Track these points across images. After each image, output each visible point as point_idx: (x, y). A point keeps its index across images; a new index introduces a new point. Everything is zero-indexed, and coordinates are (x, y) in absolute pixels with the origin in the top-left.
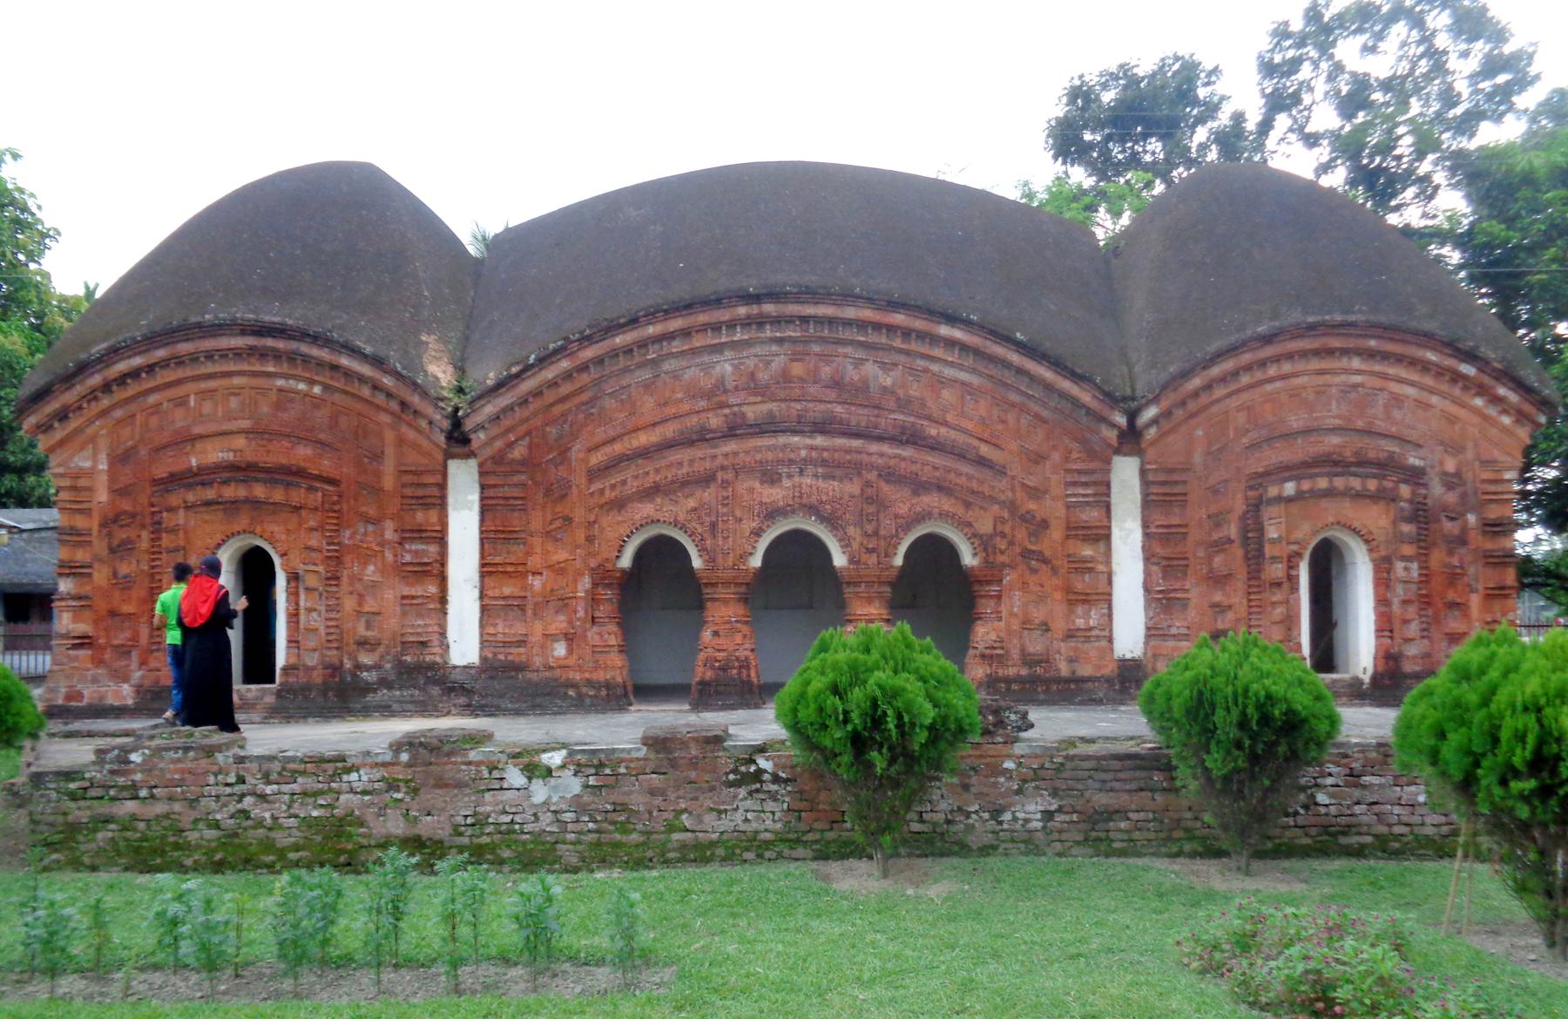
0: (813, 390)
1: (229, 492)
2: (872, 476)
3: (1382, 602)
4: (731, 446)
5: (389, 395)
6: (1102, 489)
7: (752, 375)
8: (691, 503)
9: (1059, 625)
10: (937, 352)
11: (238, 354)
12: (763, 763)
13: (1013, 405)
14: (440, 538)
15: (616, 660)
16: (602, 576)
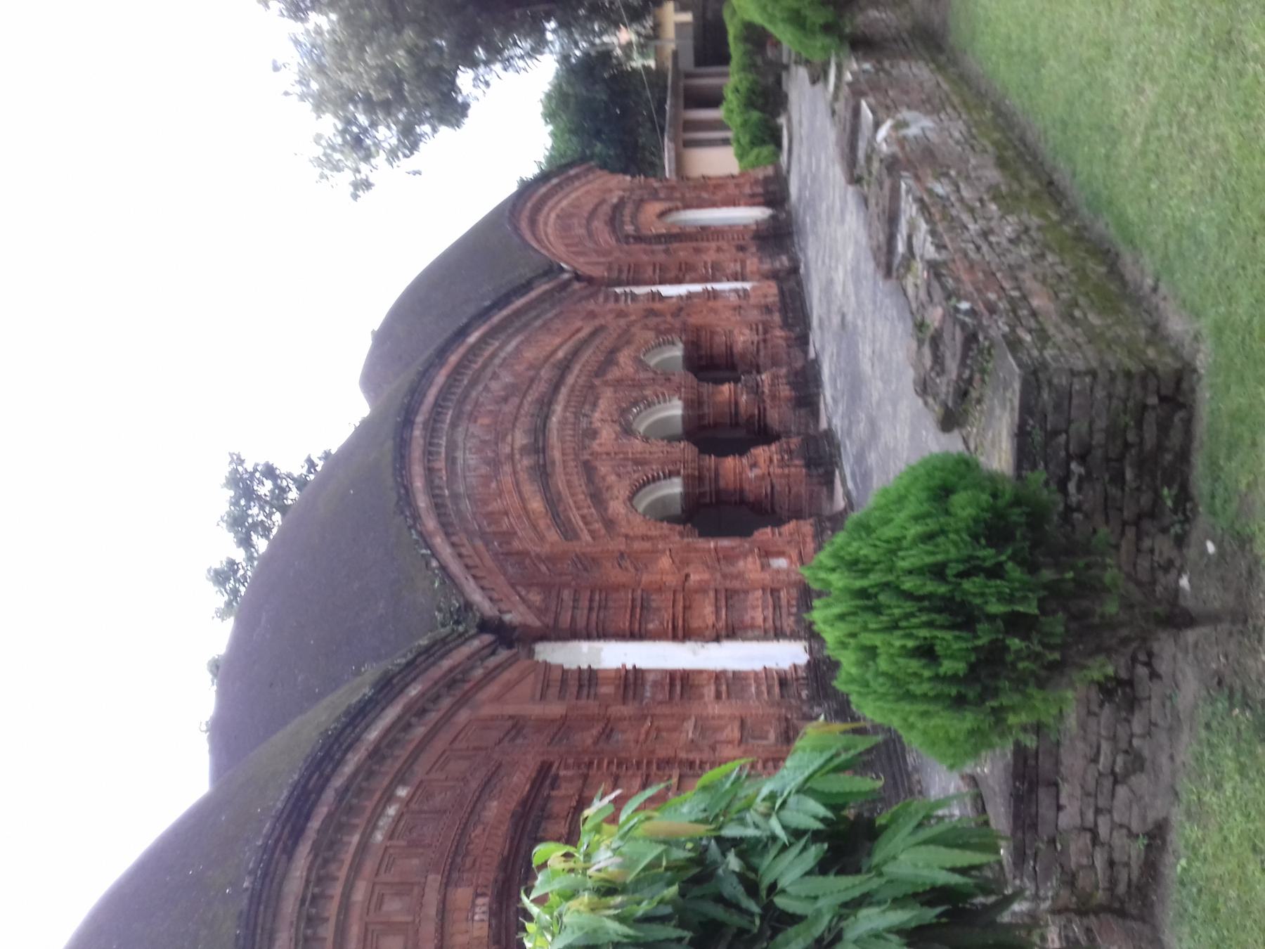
2: (597, 382)
3: (714, 204)
8: (612, 478)
10: (490, 349)
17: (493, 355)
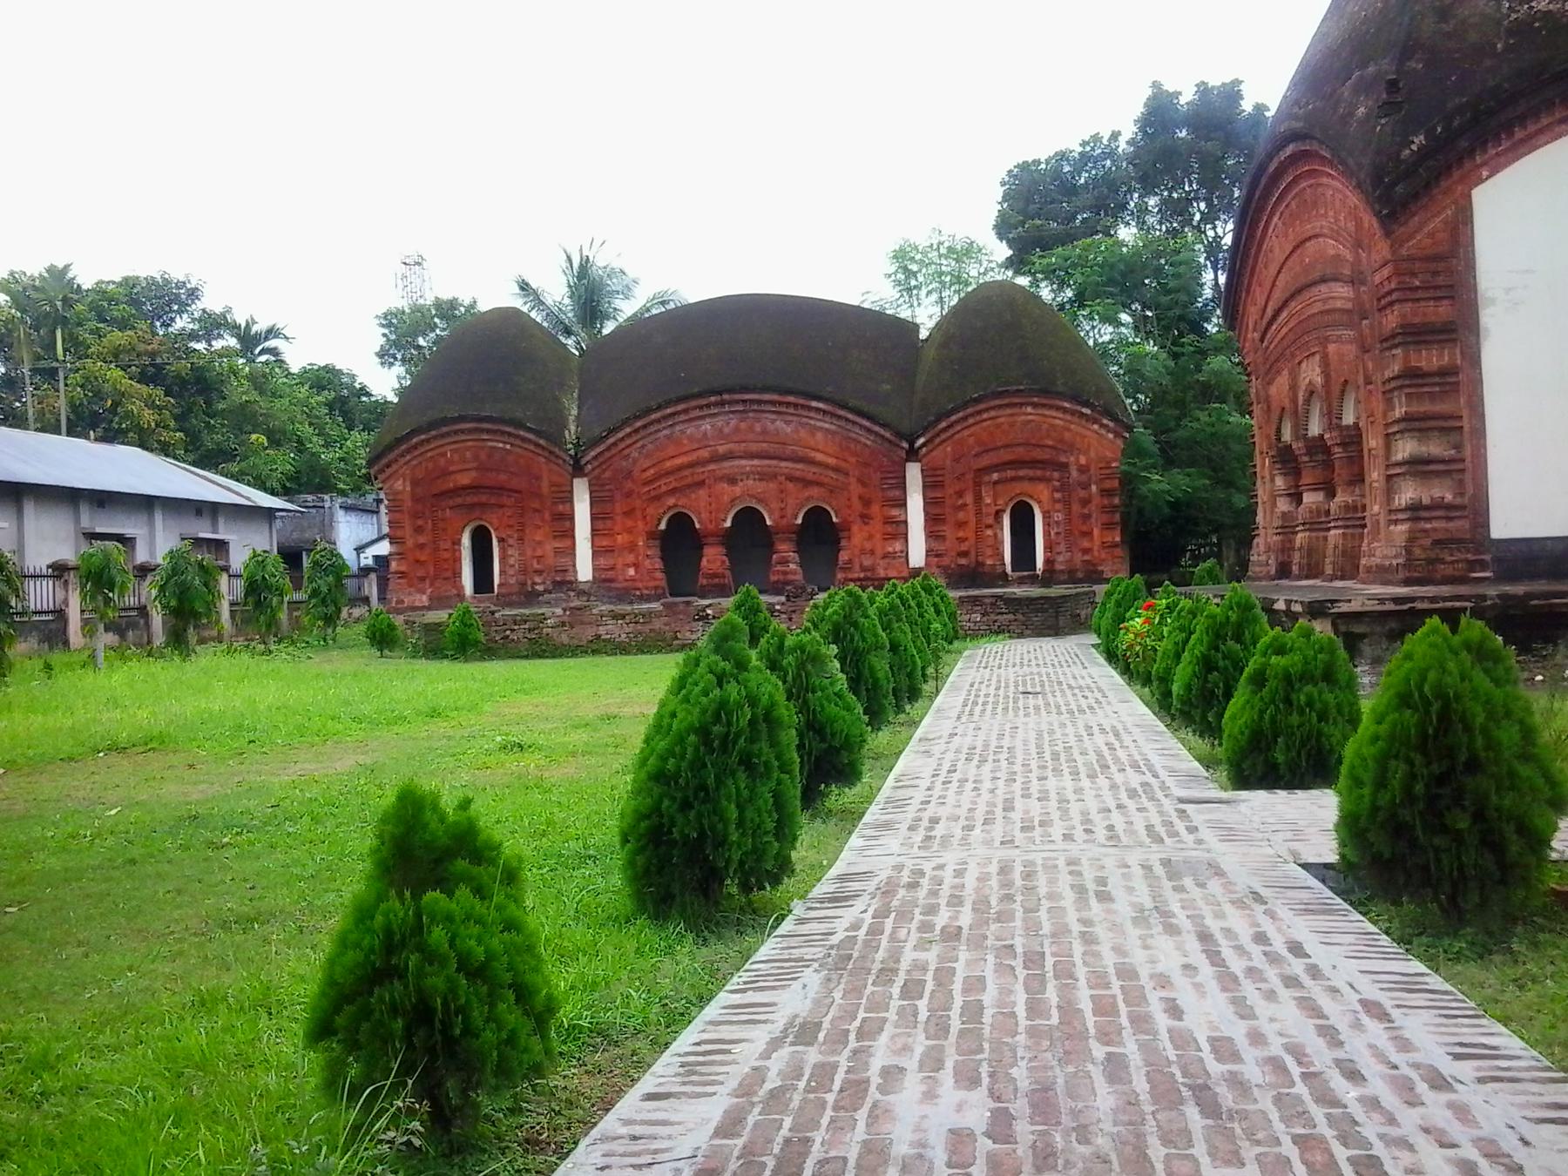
0: (751, 436)
1: (469, 500)
3: (1047, 534)
4: (712, 467)
5: (543, 448)
6: (900, 480)
7: (721, 430)
9: (879, 552)
10: (812, 414)
11: (470, 431)
12: (709, 612)
13: (854, 440)
14: (571, 518)
15: (659, 575)
16: (651, 535)
17: (811, 418)
